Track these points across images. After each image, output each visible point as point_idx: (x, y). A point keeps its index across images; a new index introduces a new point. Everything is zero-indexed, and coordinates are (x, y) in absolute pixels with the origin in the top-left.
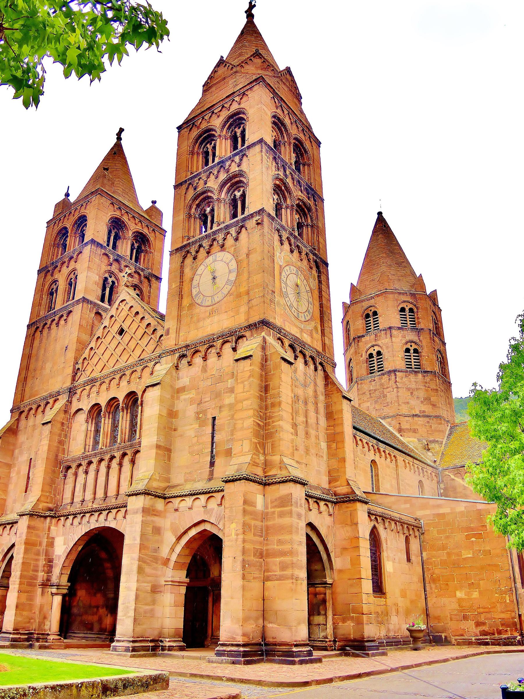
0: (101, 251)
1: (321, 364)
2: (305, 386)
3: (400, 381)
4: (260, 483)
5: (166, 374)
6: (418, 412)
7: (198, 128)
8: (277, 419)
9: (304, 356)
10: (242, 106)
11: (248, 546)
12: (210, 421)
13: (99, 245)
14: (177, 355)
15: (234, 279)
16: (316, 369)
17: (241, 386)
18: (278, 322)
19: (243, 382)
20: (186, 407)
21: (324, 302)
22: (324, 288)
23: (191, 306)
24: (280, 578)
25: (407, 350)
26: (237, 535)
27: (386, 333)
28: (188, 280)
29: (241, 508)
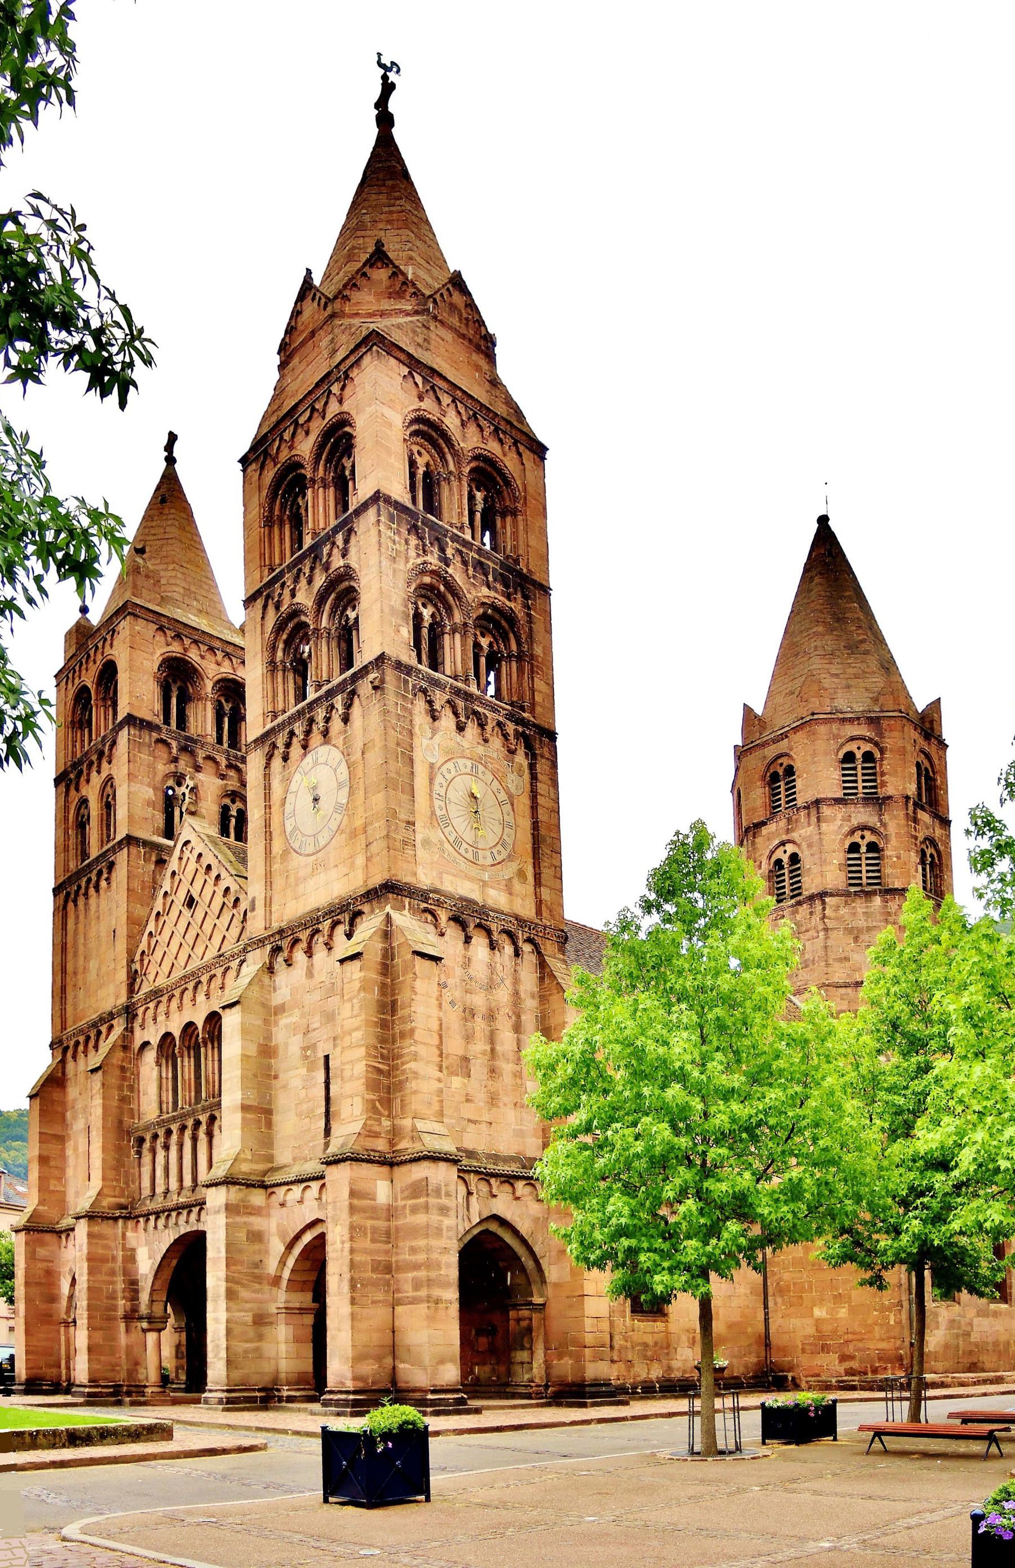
0: (150, 736)
1: (529, 940)
2: (491, 986)
4: (383, 1163)
5: (250, 983)
8: (406, 1059)
9: (489, 932)
11: (358, 1258)
13: (147, 726)
15: (345, 801)
16: (517, 953)
17: (348, 1006)
18: (424, 878)
20: (289, 1041)
21: (543, 815)
22: (542, 788)
23: (285, 853)
24: (414, 1301)
25: (854, 848)
26: (343, 1242)
27: (809, 814)
28: (278, 803)
29: (347, 1203)
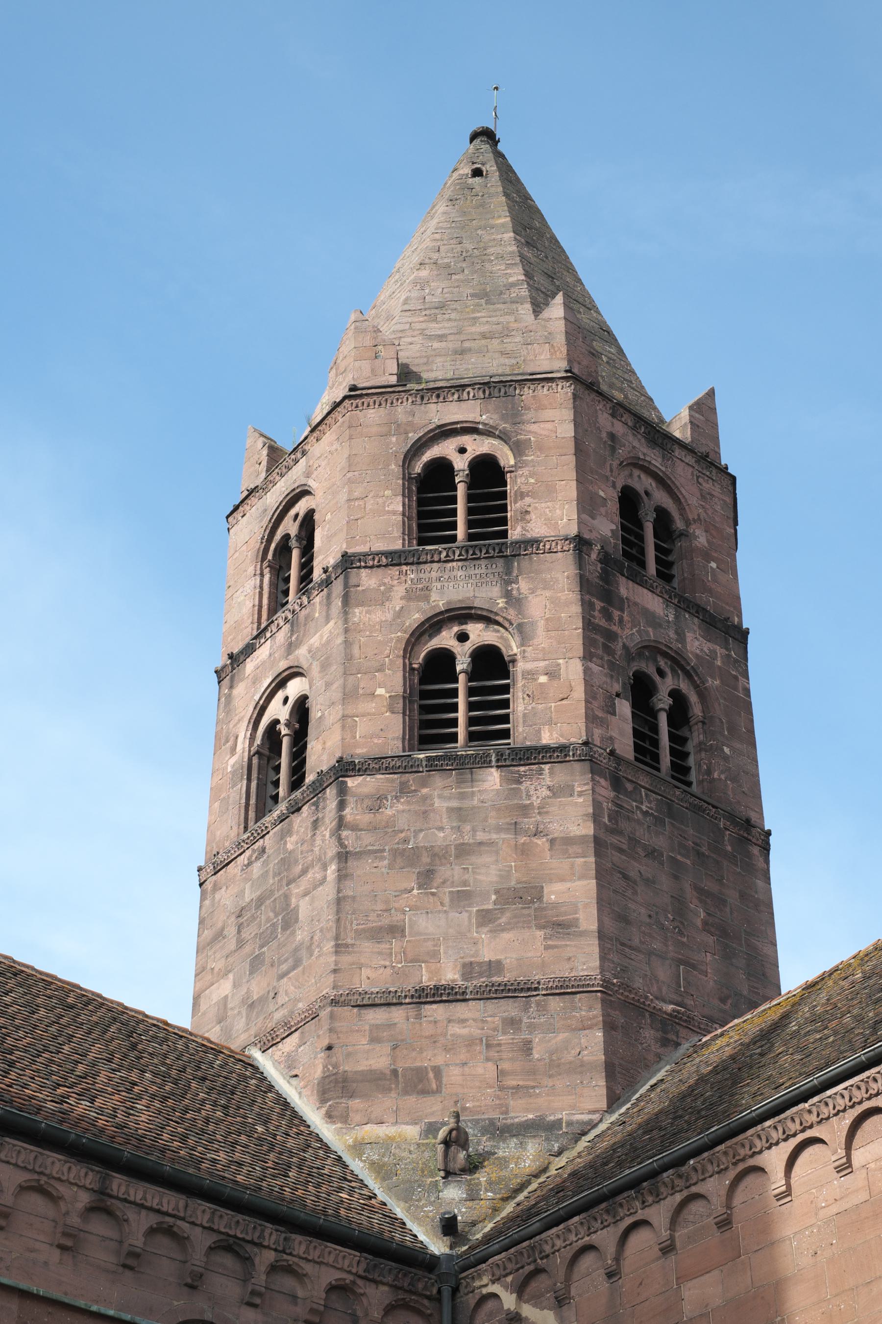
3: (365, 818)
6: (450, 975)
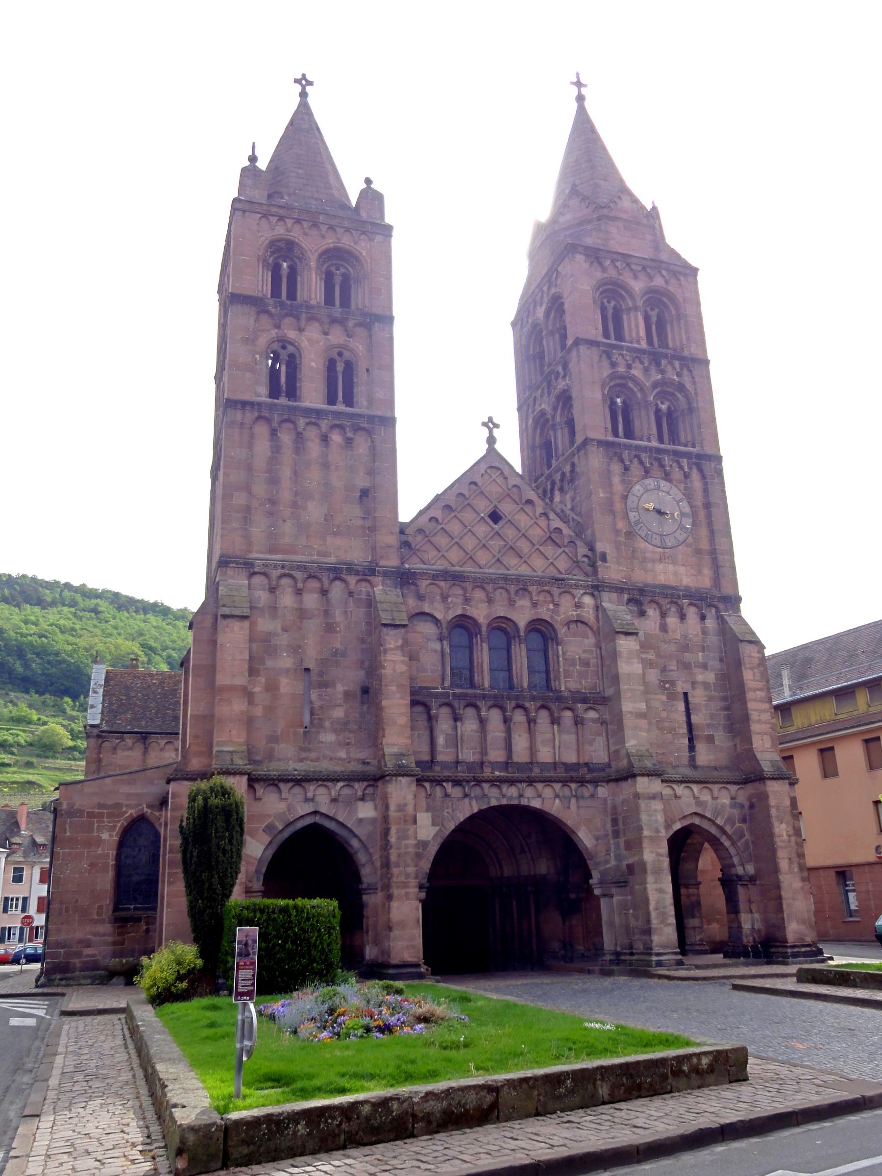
7: (604, 270)
10: (671, 288)
12: (682, 696)
14: (626, 597)
19: (751, 669)
23: (630, 535)
26: (789, 836)
